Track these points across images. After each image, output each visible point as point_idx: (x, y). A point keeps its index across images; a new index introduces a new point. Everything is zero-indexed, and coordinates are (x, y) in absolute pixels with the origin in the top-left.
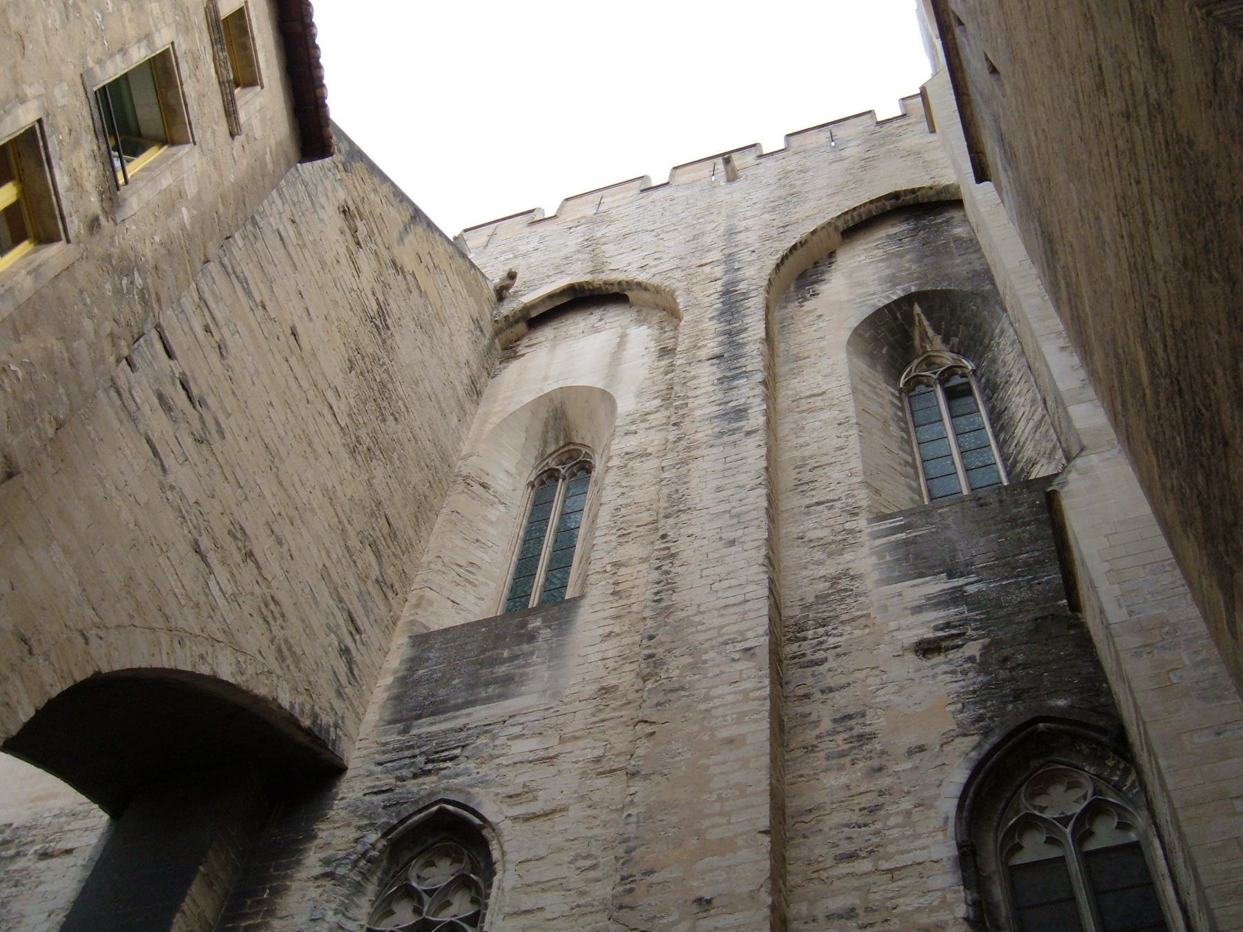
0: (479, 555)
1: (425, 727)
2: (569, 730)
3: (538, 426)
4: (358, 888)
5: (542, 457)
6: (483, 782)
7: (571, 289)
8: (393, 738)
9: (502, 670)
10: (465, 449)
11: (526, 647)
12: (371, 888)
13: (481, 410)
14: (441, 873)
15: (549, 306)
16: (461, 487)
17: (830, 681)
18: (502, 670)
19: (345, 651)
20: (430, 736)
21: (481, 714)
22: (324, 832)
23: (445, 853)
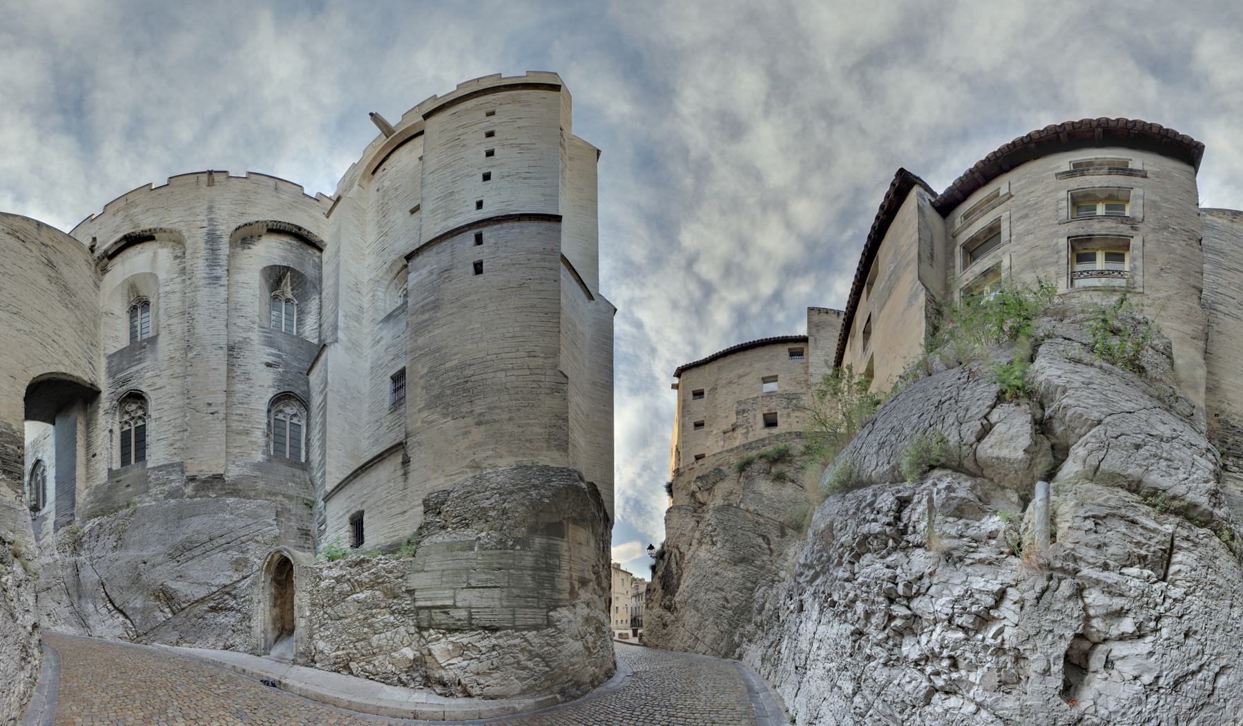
0: (117, 334)
1: (119, 376)
2: (162, 368)
3: (126, 292)
4: (114, 414)
5: (129, 302)
6: (140, 384)
7: (125, 238)
8: (111, 381)
9: (138, 357)
10: (101, 305)
11: (143, 350)
12: (118, 414)
13: (102, 292)
14: (134, 407)
15: (116, 247)
16: (105, 315)
17: (240, 363)
18: (138, 357)
19: (90, 363)
20: (121, 378)
21: (134, 369)
22: (101, 405)
23: (134, 403)
